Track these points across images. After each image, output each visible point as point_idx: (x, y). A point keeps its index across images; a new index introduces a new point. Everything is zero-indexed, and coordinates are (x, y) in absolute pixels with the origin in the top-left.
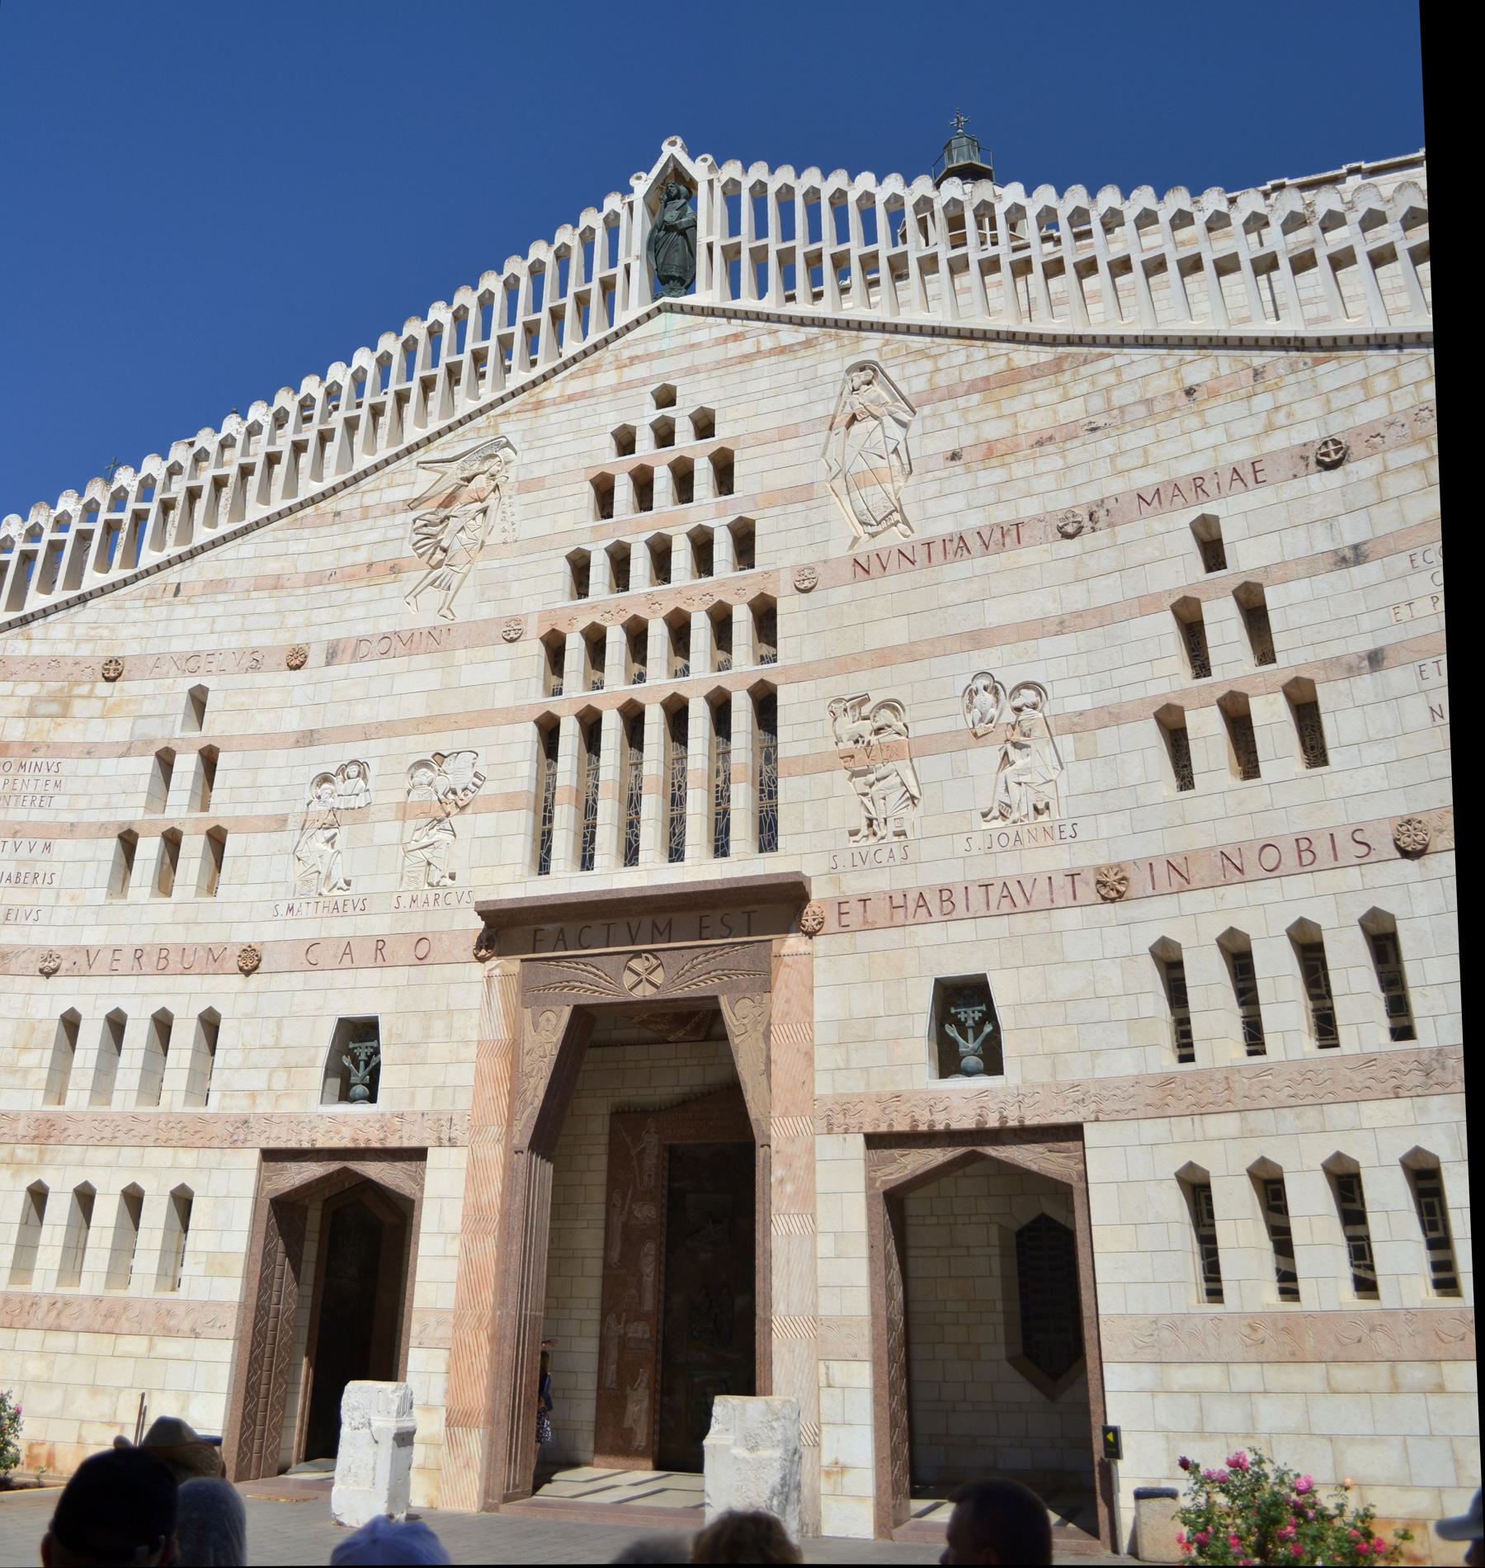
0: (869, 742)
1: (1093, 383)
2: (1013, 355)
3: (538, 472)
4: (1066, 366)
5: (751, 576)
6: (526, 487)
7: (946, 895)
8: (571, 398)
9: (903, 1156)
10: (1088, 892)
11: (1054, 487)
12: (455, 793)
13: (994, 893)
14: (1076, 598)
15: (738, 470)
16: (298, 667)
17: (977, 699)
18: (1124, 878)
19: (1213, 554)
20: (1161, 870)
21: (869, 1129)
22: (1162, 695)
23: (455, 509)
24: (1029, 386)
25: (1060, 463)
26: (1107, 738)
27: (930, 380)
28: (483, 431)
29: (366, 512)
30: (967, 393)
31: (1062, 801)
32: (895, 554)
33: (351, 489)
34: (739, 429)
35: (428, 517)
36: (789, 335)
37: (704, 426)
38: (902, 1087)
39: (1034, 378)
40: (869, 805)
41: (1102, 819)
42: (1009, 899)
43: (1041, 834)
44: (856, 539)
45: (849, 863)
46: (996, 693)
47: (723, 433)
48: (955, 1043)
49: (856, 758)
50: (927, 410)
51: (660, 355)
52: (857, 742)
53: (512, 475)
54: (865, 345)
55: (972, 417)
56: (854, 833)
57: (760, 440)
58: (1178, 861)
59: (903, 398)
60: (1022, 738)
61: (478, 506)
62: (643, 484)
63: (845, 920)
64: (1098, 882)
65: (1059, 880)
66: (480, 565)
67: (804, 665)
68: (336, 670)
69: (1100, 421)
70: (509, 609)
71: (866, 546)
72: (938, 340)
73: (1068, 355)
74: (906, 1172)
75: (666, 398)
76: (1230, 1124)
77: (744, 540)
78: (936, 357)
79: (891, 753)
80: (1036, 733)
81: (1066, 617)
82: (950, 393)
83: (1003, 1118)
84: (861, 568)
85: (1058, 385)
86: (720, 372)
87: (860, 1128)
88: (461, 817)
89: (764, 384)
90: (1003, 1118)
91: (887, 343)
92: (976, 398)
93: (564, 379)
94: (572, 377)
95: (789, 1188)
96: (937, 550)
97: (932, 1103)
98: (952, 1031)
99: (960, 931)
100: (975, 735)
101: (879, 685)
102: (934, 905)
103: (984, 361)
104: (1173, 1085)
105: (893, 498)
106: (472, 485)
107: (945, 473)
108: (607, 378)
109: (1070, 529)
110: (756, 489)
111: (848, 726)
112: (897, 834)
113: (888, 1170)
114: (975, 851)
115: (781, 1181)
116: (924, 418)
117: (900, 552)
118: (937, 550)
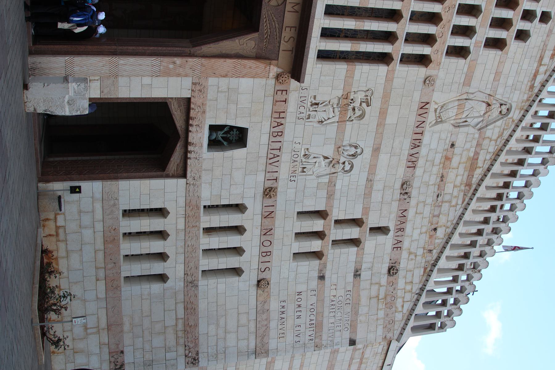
0: (350, 105)
2: (481, 169)
4: (467, 188)
5: (442, 57)
9: (181, 110)
10: (269, 184)
11: (423, 180)
13: (276, 152)
14: (378, 186)
15: (493, 53)
18: (271, 197)
20: (271, 209)
21: (192, 100)
22: (332, 213)
24: (466, 174)
25: (431, 183)
26: (323, 193)
27: (488, 138)
30: (476, 151)
31: (305, 177)
32: (423, 119)
34: (511, 54)
36: (540, 78)
37: (522, 35)
38: (208, 115)
39: (468, 176)
40: (324, 104)
41: (294, 190)
42: (273, 157)
43: (294, 169)
44: (436, 103)
45: (302, 95)
46: (353, 155)
47: (513, 46)
48: (221, 130)
49: (345, 100)
50: (477, 136)
52: (352, 100)
54: (517, 112)
55: (465, 153)
56: (315, 97)
57: (501, 63)
58: (273, 215)
59: (487, 126)
60: (332, 164)
63: (279, 93)
64: (272, 188)
65: (275, 175)
69: (440, 199)
71: (432, 107)
72: (504, 141)
73: (470, 189)
74: (174, 112)
75: (545, 17)
76: (181, 226)
78: (496, 141)
81: (372, 182)
82: (479, 145)
83: (190, 152)
84: (424, 106)
85: (461, 184)
86: (542, 46)
87: (193, 96)
89: (525, 66)
90: (190, 152)
91: (513, 121)
92: (472, 155)
95: (171, 66)
97: (200, 126)
98: (226, 129)
99: (265, 139)
100: (340, 147)
101: (372, 113)
102: (277, 129)
103: (484, 158)
104: (196, 209)
105: (447, 120)
109: (405, 186)
110: (478, 62)
111: (360, 96)
112: (309, 115)
113: (175, 104)
114: (294, 145)
115: (174, 63)
116: (474, 134)
117: (424, 122)
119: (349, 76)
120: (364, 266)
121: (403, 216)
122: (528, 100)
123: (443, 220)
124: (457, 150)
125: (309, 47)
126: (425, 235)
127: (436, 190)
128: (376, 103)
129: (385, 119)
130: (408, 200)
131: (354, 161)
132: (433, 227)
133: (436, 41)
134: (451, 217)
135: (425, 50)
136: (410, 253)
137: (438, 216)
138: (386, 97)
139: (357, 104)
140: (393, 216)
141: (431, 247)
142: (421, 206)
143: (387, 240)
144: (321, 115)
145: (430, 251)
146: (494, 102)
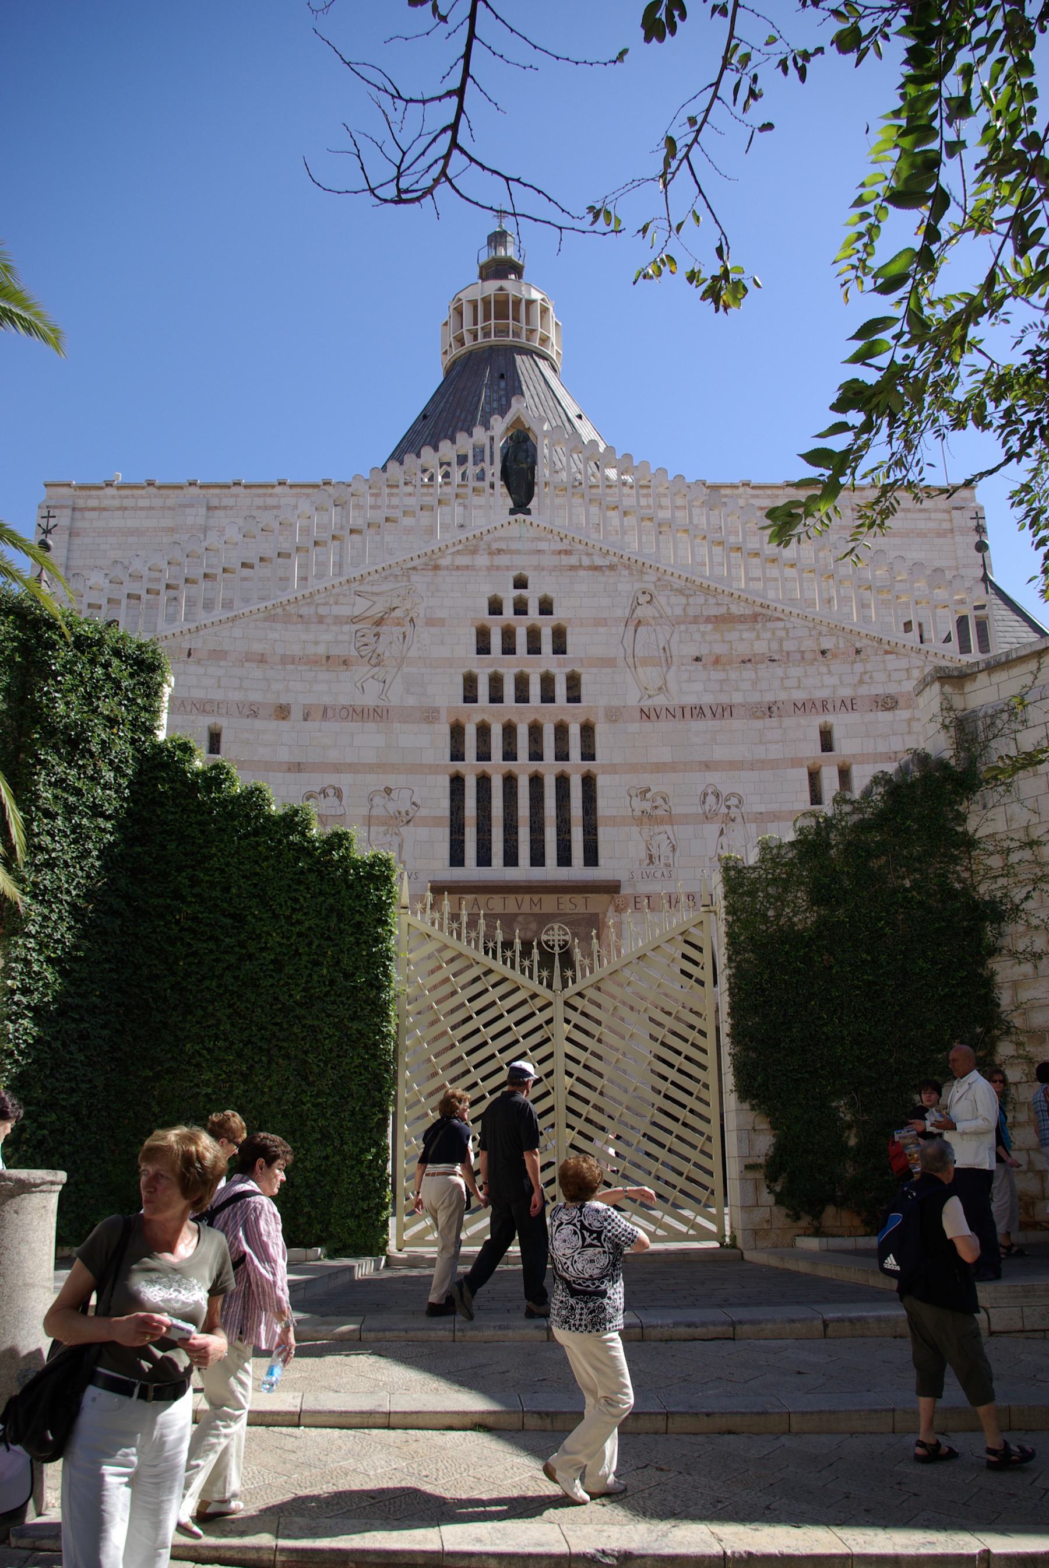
1: (773, 633)
2: (731, 606)
4: (759, 619)
7: (691, 898)
8: (458, 568)
12: (399, 813)
16: (283, 718)
17: (708, 798)
19: (827, 742)
23: (383, 629)
27: (684, 609)
28: (399, 578)
29: (321, 619)
32: (664, 710)
33: (308, 601)
35: (365, 631)
46: (717, 797)
47: (560, 613)
50: (683, 627)
51: (517, 552)
53: (422, 615)
54: (646, 578)
62: (508, 635)
66: (406, 670)
67: (614, 765)
68: (309, 724)
71: (647, 703)
75: (521, 583)
77: (574, 682)
79: (660, 821)
80: (737, 821)
82: (695, 620)
84: (645, 714)
88: (406, 828)
92: (710, 626)
93: (453, 554)
101: (658, 783)
106: (394, 614)
107: (693, 668)
108: (482, 560)
109: (759, 714)
111: (637, 803)
116: (681, 632)
119: (614, 821)
120: (881, 749)
121: (803, 707)
122: (628, 567)
123: (809, 644)
124: (704, 651)
125: (576, 881)
126: (831, 667)
127: (763, 666)
128: (645, 779)
129: (665, 764)
130: (780, 705)
131: (725, 793)
132: (820, 657)
135: (574, 731)
136: (861, 682)
137: (803, 652)
138: (634, 768)
139: (647, 806)
140: (803, 721)
141: (852, 651)
142: (788, 683)
143: (840, 723)
144: (665, 849)
146: (635, 616)
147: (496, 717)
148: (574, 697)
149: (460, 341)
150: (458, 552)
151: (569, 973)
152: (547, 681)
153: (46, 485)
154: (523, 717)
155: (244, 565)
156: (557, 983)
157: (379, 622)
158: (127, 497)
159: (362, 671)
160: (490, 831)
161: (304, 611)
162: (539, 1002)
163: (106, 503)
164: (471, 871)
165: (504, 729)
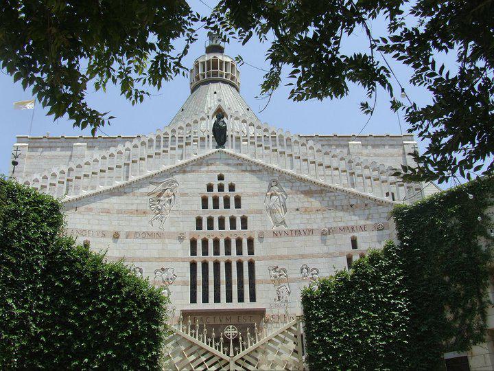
3: (186, 192)
6: (182, 195)
12: (168, 279)
14: (325, 249)
15: (243, 202)
19: (354, 245)
23: (162, 198)
34: (242, 191)
37: (232, 188)
47: (238, 191)
50: (290, 196)
54: (274, 175)
56: (275, 300)
61: (168, 199)
62: (216, 200)
68: (128, 240)
70: (181, 230)
71: (275, 228)
75: (221, 178)
77: (244, 220)
79: (283, 281)
84: (275, 234)
94: (194, 165)
96: (294, 234)
101: (281, 264)
111: (273, 273)
118: (294, 234)
121: (343, 230)
122: (266, 170)
123: (345, 202)
124: (300, 206)
133: (239, 237)
134: (343, 197)
135: (245, 242)
137: (343, 206)
138: (272, 258)
143: (360, 236)
145: (366, 205)
147: (210, 236)
148: (244, 226)
149: (198, 78)
150: (194, 165)
151: (237, 349)
152: (233, 220)
153: (18, 137)
154: (222, 236)
155: (102, 171)
156: (232, 354)
157: (160, 195)
158: (52, 142)
159: (151, 216)
160: (208, 287)
161: (126, 190)
162: (223, 363)
163: (43, 145)
164: (200, 305)
165: (214, 242)
